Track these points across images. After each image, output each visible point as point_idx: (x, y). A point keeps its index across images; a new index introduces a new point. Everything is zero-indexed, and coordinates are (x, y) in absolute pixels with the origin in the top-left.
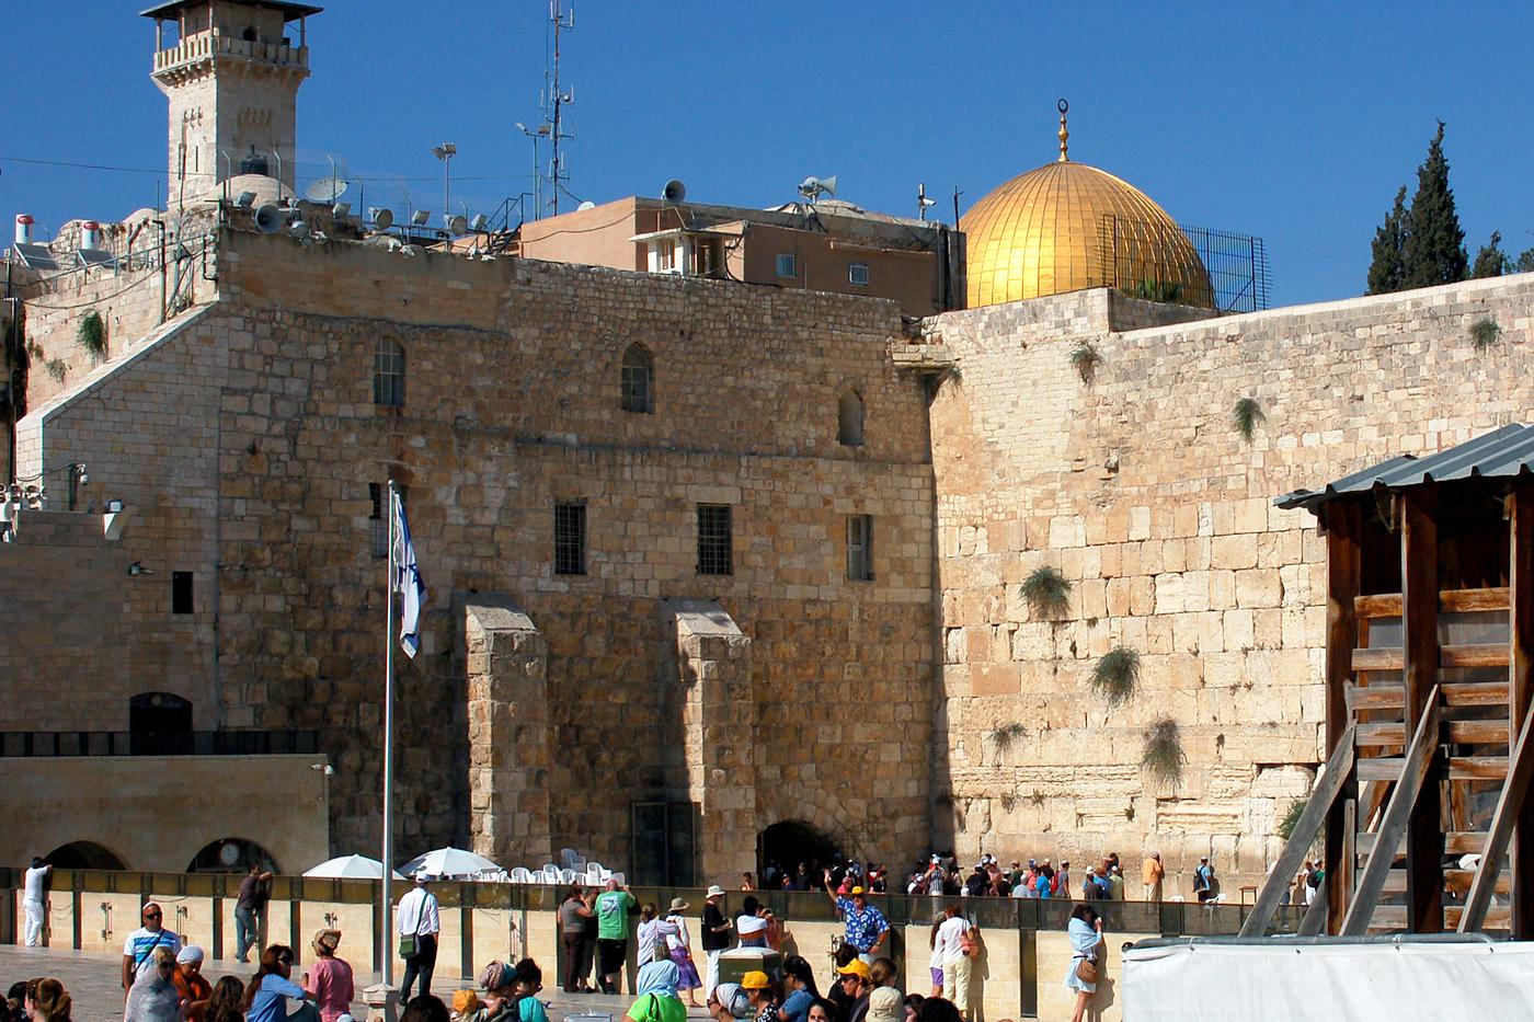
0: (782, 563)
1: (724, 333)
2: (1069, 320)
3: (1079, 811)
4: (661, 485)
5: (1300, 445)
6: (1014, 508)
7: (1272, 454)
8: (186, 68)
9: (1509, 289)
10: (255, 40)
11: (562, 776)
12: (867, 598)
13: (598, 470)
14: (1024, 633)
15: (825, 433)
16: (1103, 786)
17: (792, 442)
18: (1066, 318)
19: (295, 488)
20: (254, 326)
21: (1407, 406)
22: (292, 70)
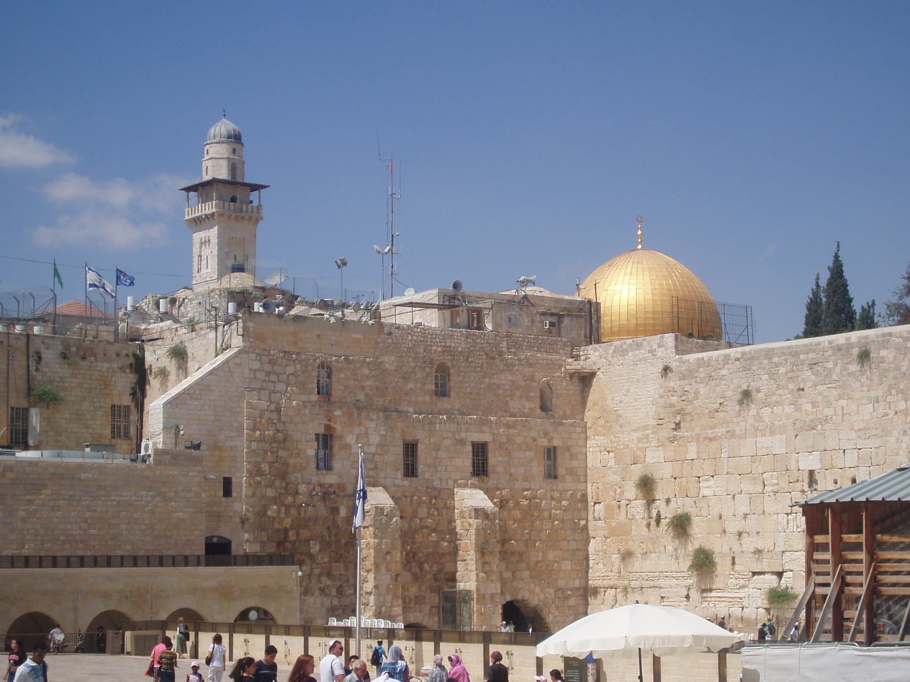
0: (513, 470)
1: (484, 357)
4: (454, 433)
5: (772, 412)
7: (759, 418)
9: (877, 336)
11: (406, 577)
12: (554, 487)
13: (424, 425)
14: (633, 505)
15: (533, 405)
16: (675, 581)
17: (517, 410)
18: (654, 348)
19: (280, 436)
20: (261, 358)
21: (826, 393)
22: (255, 218)
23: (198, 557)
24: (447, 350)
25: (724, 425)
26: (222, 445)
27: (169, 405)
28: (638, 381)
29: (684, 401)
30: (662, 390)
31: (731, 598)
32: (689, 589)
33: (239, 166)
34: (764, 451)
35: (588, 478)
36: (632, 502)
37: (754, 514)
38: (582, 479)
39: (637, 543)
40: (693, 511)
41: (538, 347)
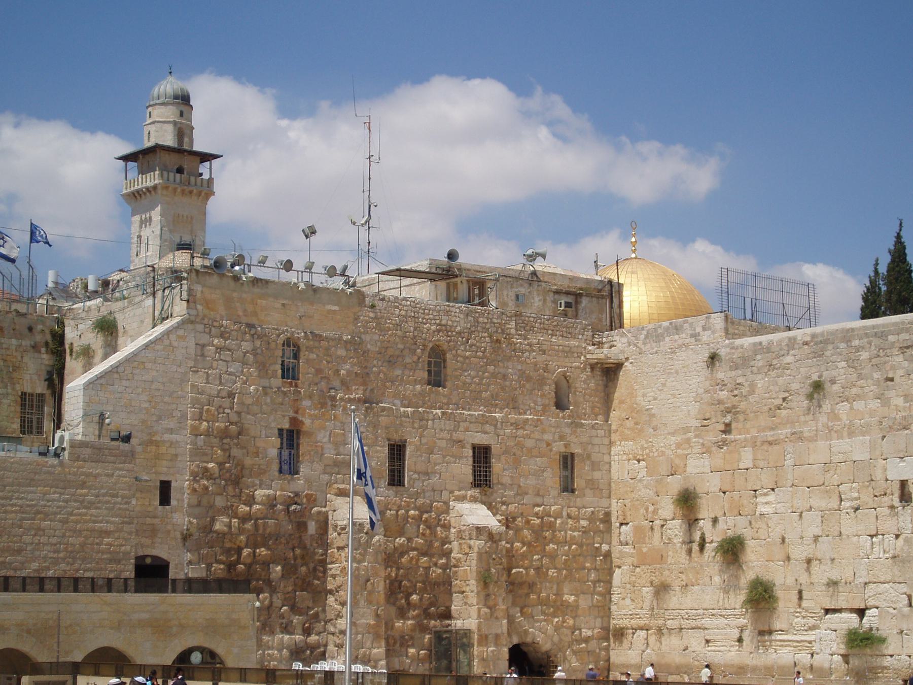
2: (699, 333)
3: (708, 638)
5: (852, 408)
6: (663, 449)
8: (142, 190)
10: (183, 174)
13: (413, 422)
14: (670, 526)
15: (547, 402)
16: (723, 621)
18: (697, 331)
23: (126, 580)
24: (443, 328)
25: (789, 426)
26: (159, 439)
27: (91, 386)
28: (677, 372)
29: (736, 396)
30: (708, 383)
31: (798, 642)
32: (742, 630)
33: (187, 131)
34: (841, 457)
35: (613, 493)
36: (668, 522)
37: (827, 536)
38: (605, 493)
39: (675, 572)
40: (747, 533)
41: (553, 330)
